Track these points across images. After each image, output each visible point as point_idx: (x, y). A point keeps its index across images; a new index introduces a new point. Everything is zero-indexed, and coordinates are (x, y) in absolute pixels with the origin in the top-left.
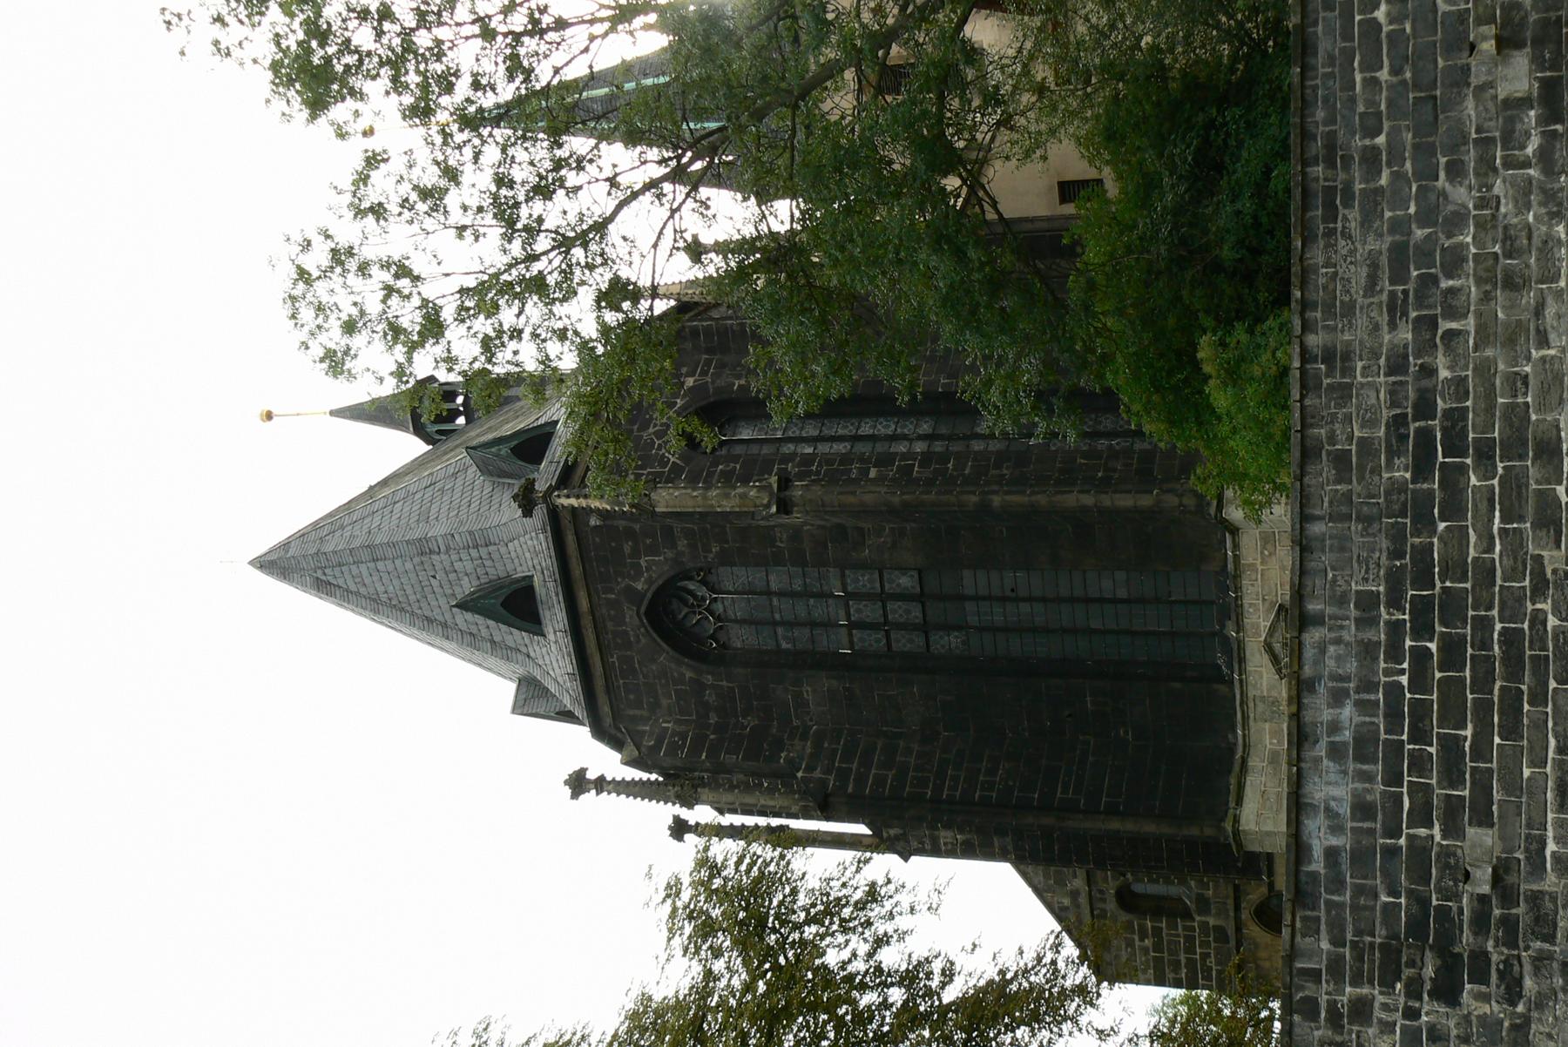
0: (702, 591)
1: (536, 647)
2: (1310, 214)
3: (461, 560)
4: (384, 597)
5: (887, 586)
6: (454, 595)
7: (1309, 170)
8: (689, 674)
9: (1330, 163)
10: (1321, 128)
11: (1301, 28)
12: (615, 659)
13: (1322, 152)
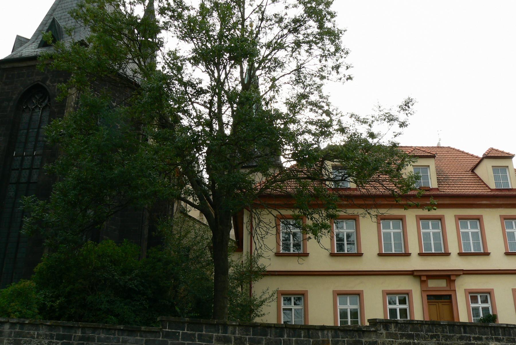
0: (44, 104)
1: (36, 44)
2: (61, 329)
3: (72, 23)
5: (35, 170)
6: (61, 19)
7: (80, 330)
8: (14, 97)
9: (81, 338)
10: (97, 336)
11: (140, 331)
12: (24, 71)
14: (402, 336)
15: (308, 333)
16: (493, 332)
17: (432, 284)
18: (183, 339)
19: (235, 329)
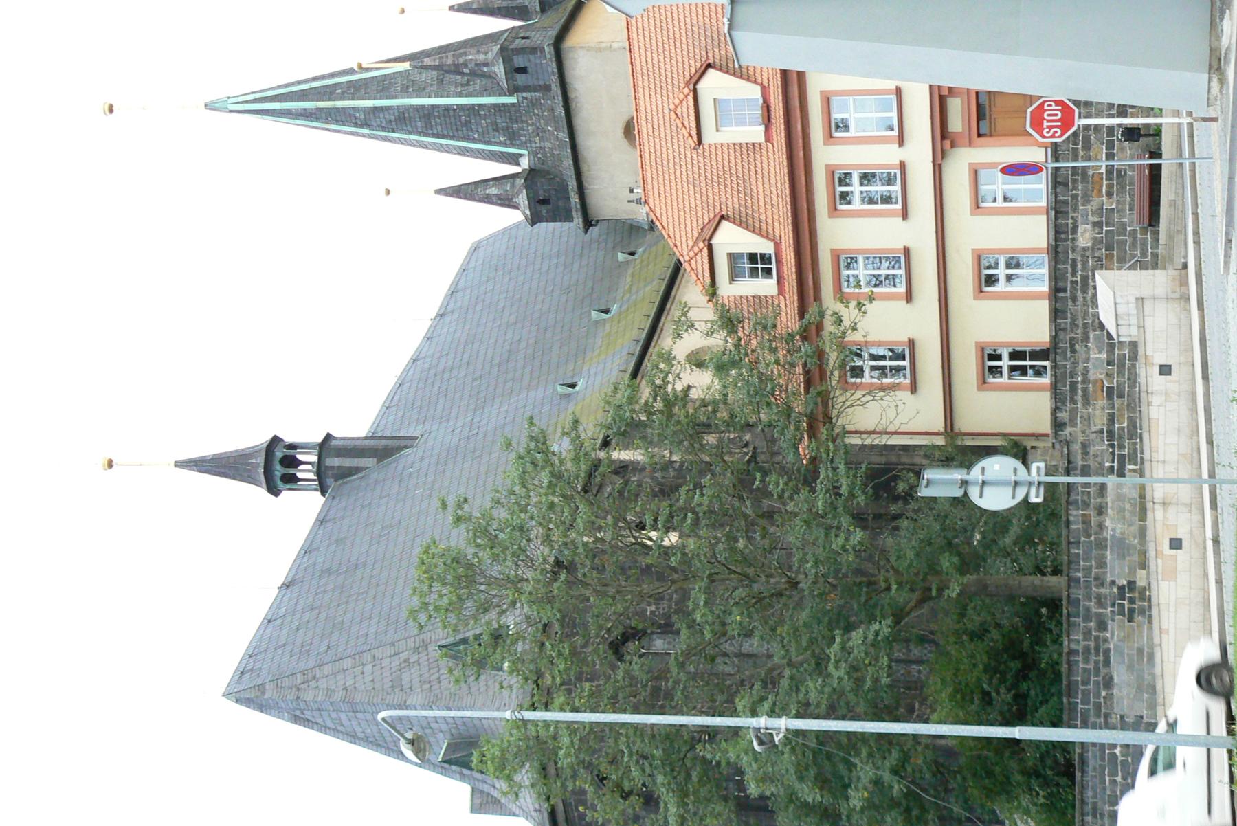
4: (359, 735)
9: (1095, 816)
13: (1091, 811)
14: (1073, 401)
15: (1073, 543)
16: (1063, 236)
17: (956, 123)
18: (1088, 704)
19: (1072, 640)
